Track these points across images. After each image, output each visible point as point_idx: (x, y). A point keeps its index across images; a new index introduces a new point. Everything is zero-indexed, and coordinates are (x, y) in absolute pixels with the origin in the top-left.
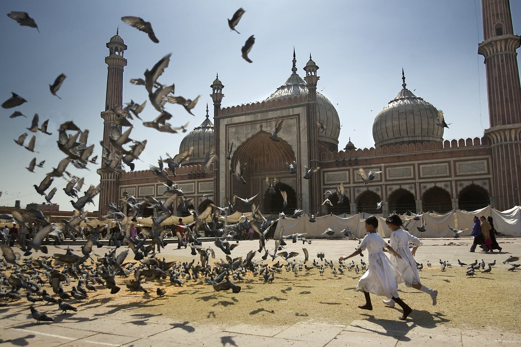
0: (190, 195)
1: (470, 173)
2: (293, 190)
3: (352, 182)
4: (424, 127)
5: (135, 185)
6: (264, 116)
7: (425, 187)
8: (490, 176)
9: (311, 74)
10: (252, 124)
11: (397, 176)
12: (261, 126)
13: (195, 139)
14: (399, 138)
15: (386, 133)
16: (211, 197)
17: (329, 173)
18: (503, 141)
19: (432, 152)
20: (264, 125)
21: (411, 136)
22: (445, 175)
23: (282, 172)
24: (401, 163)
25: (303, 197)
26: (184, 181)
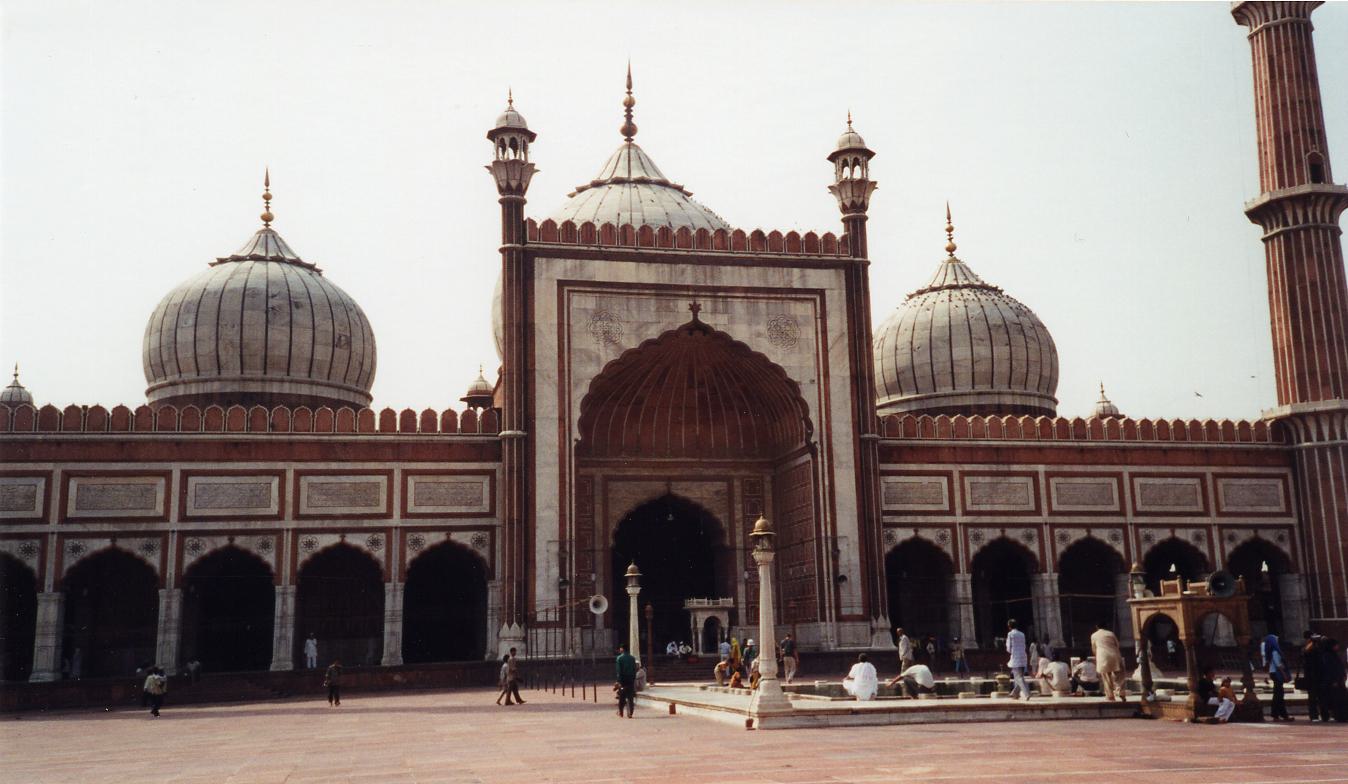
0: (366, 523)
1: (1249, 509)
2: (717, 522)
3: (959, 511)
4: (1043, 373)
5: (49, 466)
6: (705, 276)
7: (1148, 538)
8: (1293, 521)
9: (852, 171)
10: (662, 295)
11: (1078, 504)
12: (695, 309)
13: (273, 302)
14: (989, 393)
15: (949, 378)
16: (464, 534)
17: (891, 479)
18: (1338, 436)
19: (1164, 445)
20: (705, 304)
21: (1018, 391)
22: (1194, 509)
23: (679, 460)
24: (1089, 469)
25: (842, 546)
26: (334, 466)
